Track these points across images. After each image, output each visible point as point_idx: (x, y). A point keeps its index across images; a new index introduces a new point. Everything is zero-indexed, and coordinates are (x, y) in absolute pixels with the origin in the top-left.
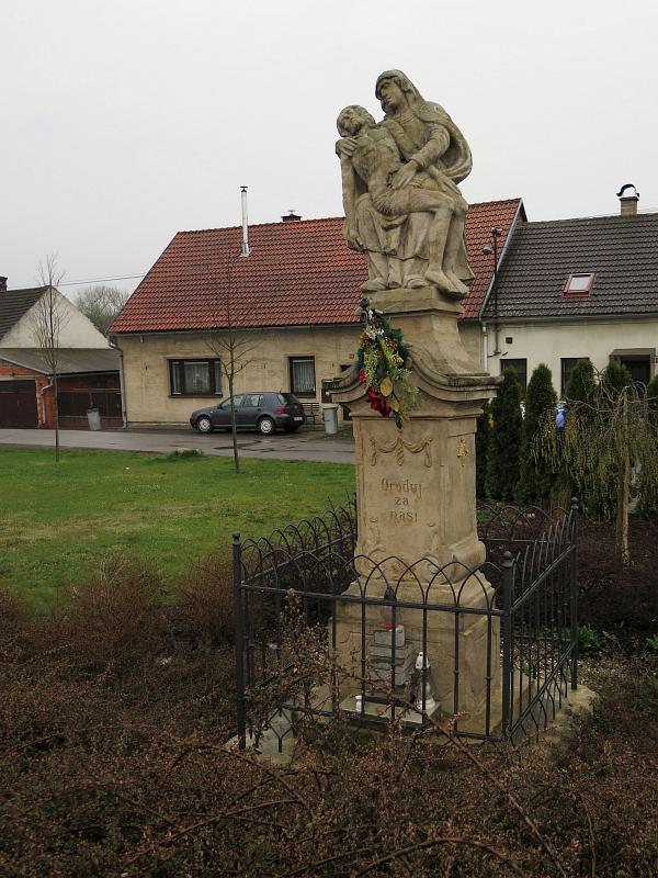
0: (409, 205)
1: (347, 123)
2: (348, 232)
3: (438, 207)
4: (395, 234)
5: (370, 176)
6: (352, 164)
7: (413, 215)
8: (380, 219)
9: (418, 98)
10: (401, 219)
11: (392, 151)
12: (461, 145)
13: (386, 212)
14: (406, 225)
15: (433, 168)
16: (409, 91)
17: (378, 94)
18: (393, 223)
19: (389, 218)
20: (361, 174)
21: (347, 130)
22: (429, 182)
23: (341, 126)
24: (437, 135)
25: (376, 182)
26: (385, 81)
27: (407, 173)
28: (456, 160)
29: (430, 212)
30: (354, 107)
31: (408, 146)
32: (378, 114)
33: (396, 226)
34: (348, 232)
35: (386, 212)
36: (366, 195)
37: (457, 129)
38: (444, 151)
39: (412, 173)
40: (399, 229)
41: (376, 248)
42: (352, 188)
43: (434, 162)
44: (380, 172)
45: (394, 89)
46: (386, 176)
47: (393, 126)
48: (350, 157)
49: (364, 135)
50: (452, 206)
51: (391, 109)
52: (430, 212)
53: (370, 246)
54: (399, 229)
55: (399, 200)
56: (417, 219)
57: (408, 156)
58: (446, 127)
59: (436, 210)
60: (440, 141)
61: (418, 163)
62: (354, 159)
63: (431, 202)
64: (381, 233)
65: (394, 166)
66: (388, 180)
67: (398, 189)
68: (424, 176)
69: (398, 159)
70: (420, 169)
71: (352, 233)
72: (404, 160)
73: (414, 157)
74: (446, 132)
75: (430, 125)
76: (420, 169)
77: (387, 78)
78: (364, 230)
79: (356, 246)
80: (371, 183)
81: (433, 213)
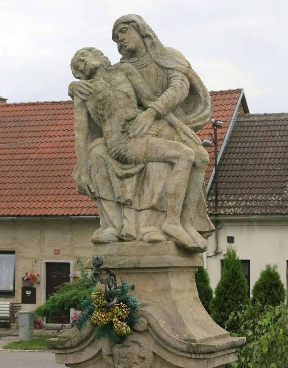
0: (146, 154)
1: (82, 66)
2: (79, 177)
3: (177, 158)
4: (130, 184)
5: (104, 121)
6: (86, 106)
7: (149, 165)
8: (117, 168)
9: (155, 44)
10: (139, 167)
11: (129, 97)
12: (201, 93)
13: (122, 160)
14: (142, 174)
15: (172, 117)
16: (148, 36)
17: (115, 37)
18: (129, 171)
19: (126, 166)
20: (95, 119)
21: (82, 72)
22: (168, 131)
23: (75, 67)
24: (176, 82)
25: (111, 127)
26: (123, 26)
27: (144, 119)
28: (195, 107)
29: (170, 163)
30: (90, 50)
31: (146, 91)
32: (114, 56)
33: (132, 175)
34: (79, 177)
35: (122, 160)
36: (100, 140)
37: (198, 78)
38: (183, 99)
39: (149, 121)
40: (135, 178)
41: (109, 197)
42: (86, 132)
43: (173, 109)
44: (115, 119)
45: (132, 35)
46: (122, 123)
47: (130, 71)
48: (84, 101)
49: (99, 82)
50: (192, 158)
51: (129, 53)
52: (170, 163)
53: (104, 193)
54: (135, 178)
55: (135, 148)
56: (155, 169)
57: (146, 103)
58: (186, 74)
59: (174, 161)
60: (178, 90)
61: (157, 112)
62: (88, 103)
63: (172, 152)
64: (116, 183)
65: (131, 112)
66: (124, 127)
67: (135, 137)
68: (163, 123)
69: (135, 105)
70: (158, 117)
71: (84, 179)
72: (141, 106)
73: (152, 104)
74: (186, 79)
75: (170, 71)
76: (158, 117)
77: (124, 23)
78: (98, 177)
79: (88, 192)
80: (107, 129)
81: (172, 164)
